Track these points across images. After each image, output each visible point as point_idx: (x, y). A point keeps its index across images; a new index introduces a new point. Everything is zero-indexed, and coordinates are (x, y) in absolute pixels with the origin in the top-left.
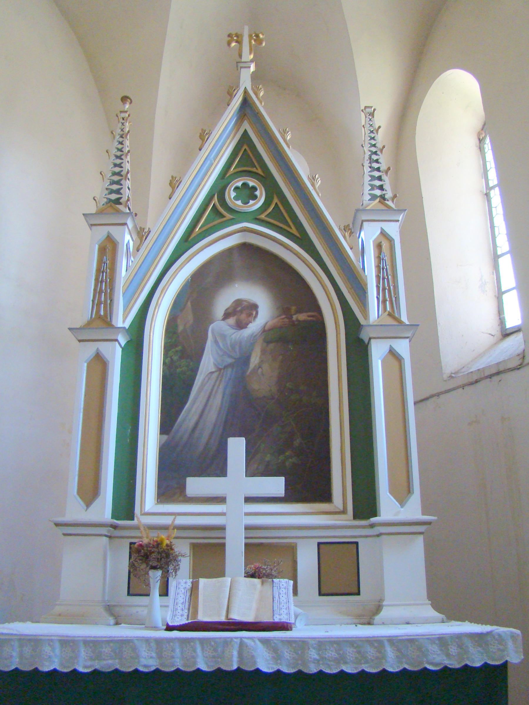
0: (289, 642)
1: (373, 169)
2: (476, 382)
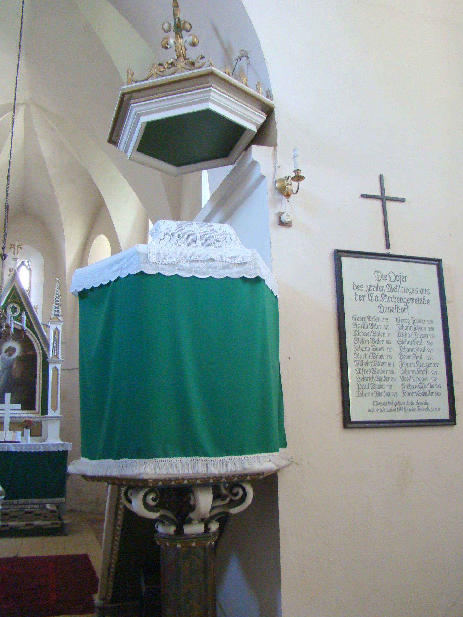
0: (19, 445)
1: (56, 304)
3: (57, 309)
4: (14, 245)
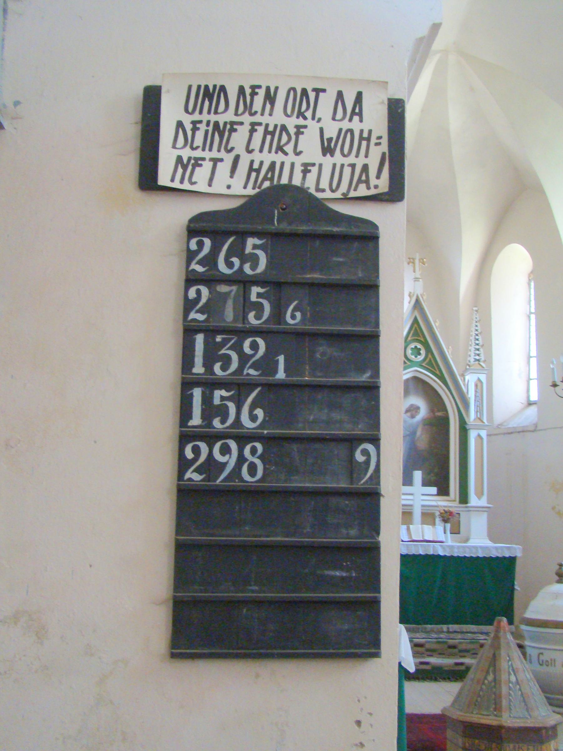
2: (512, 433)
3: (477, 352)
4: (414, 259)
